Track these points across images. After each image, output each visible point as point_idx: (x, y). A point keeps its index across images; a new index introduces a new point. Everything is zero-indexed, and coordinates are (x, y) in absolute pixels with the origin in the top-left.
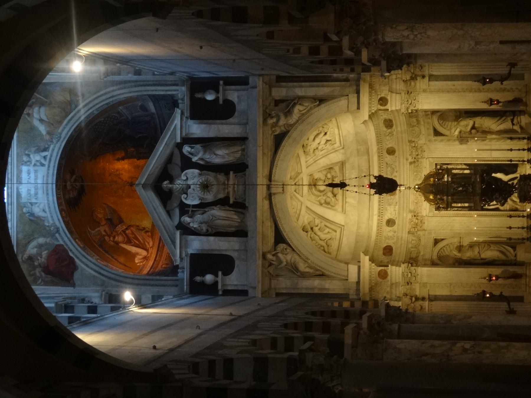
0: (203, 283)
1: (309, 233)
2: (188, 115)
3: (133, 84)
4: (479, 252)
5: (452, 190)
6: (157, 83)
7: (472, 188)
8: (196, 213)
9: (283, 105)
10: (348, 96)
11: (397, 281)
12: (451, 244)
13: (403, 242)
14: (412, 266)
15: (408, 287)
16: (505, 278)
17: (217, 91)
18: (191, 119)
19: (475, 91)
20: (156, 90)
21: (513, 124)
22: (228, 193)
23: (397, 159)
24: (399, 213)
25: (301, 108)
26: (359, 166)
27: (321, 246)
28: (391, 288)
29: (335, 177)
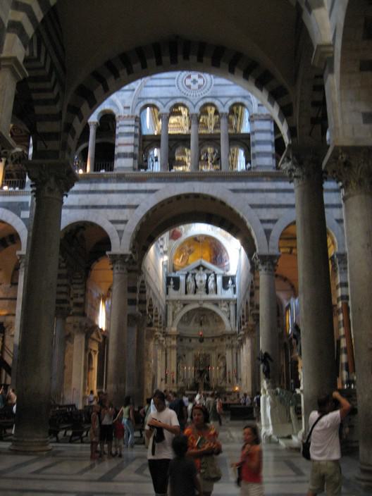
9: (227, 306)
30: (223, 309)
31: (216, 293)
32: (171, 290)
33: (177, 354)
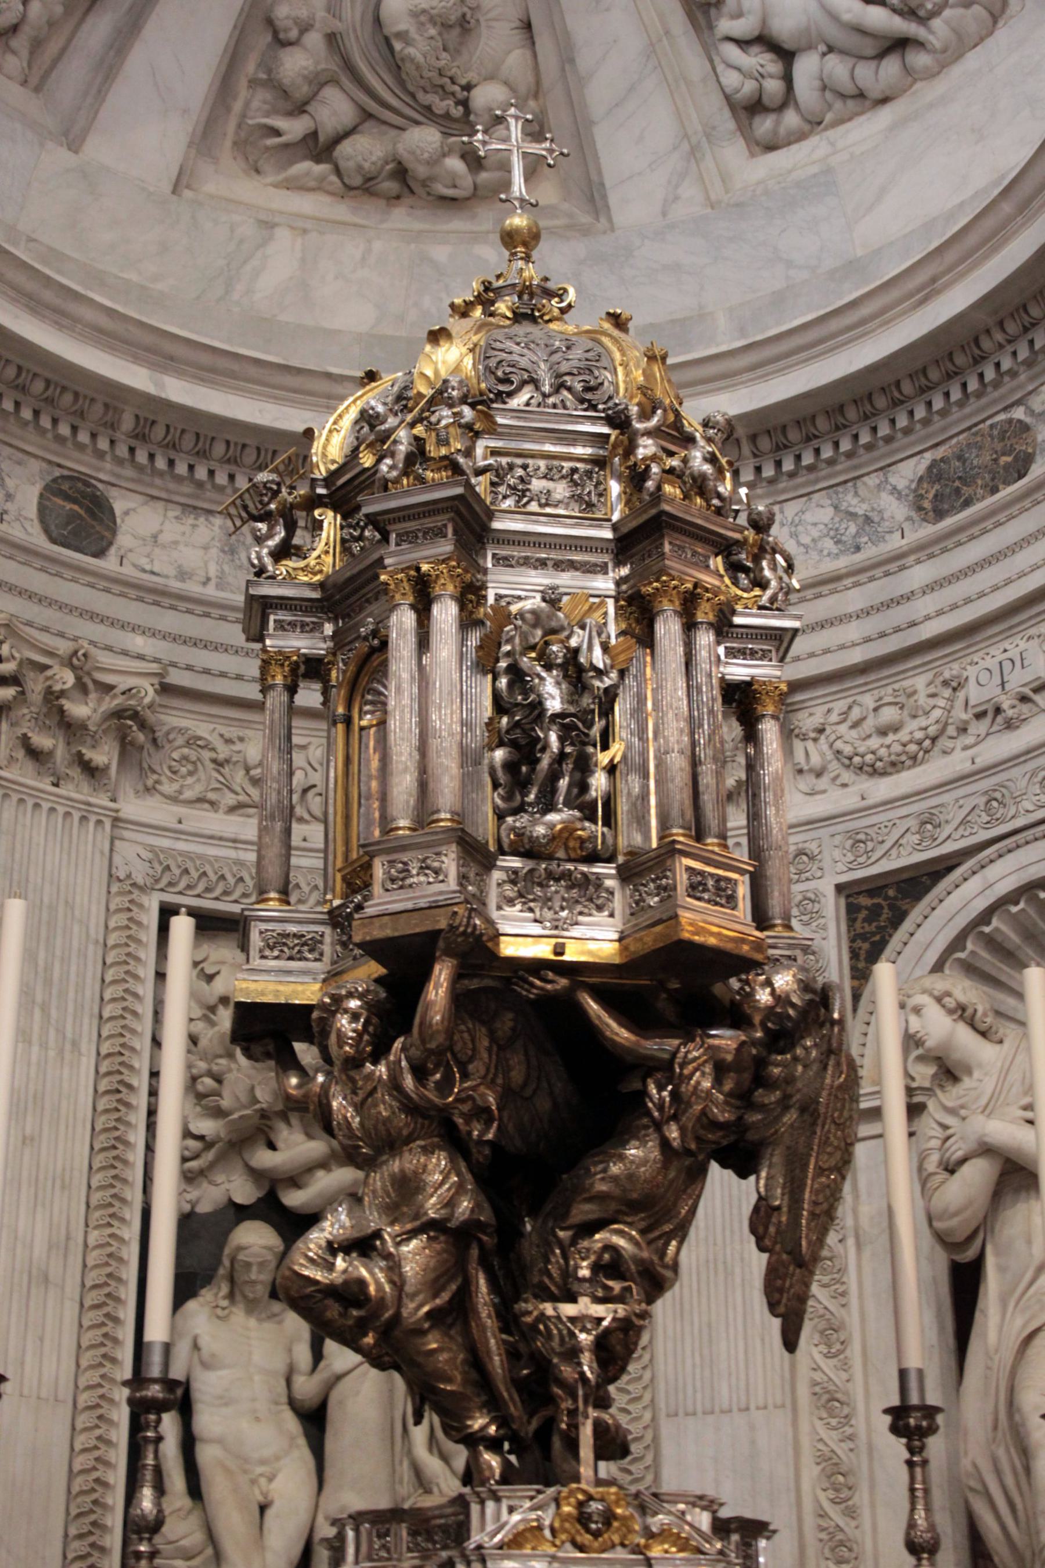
5: (535, 602)
24: (158, 595)
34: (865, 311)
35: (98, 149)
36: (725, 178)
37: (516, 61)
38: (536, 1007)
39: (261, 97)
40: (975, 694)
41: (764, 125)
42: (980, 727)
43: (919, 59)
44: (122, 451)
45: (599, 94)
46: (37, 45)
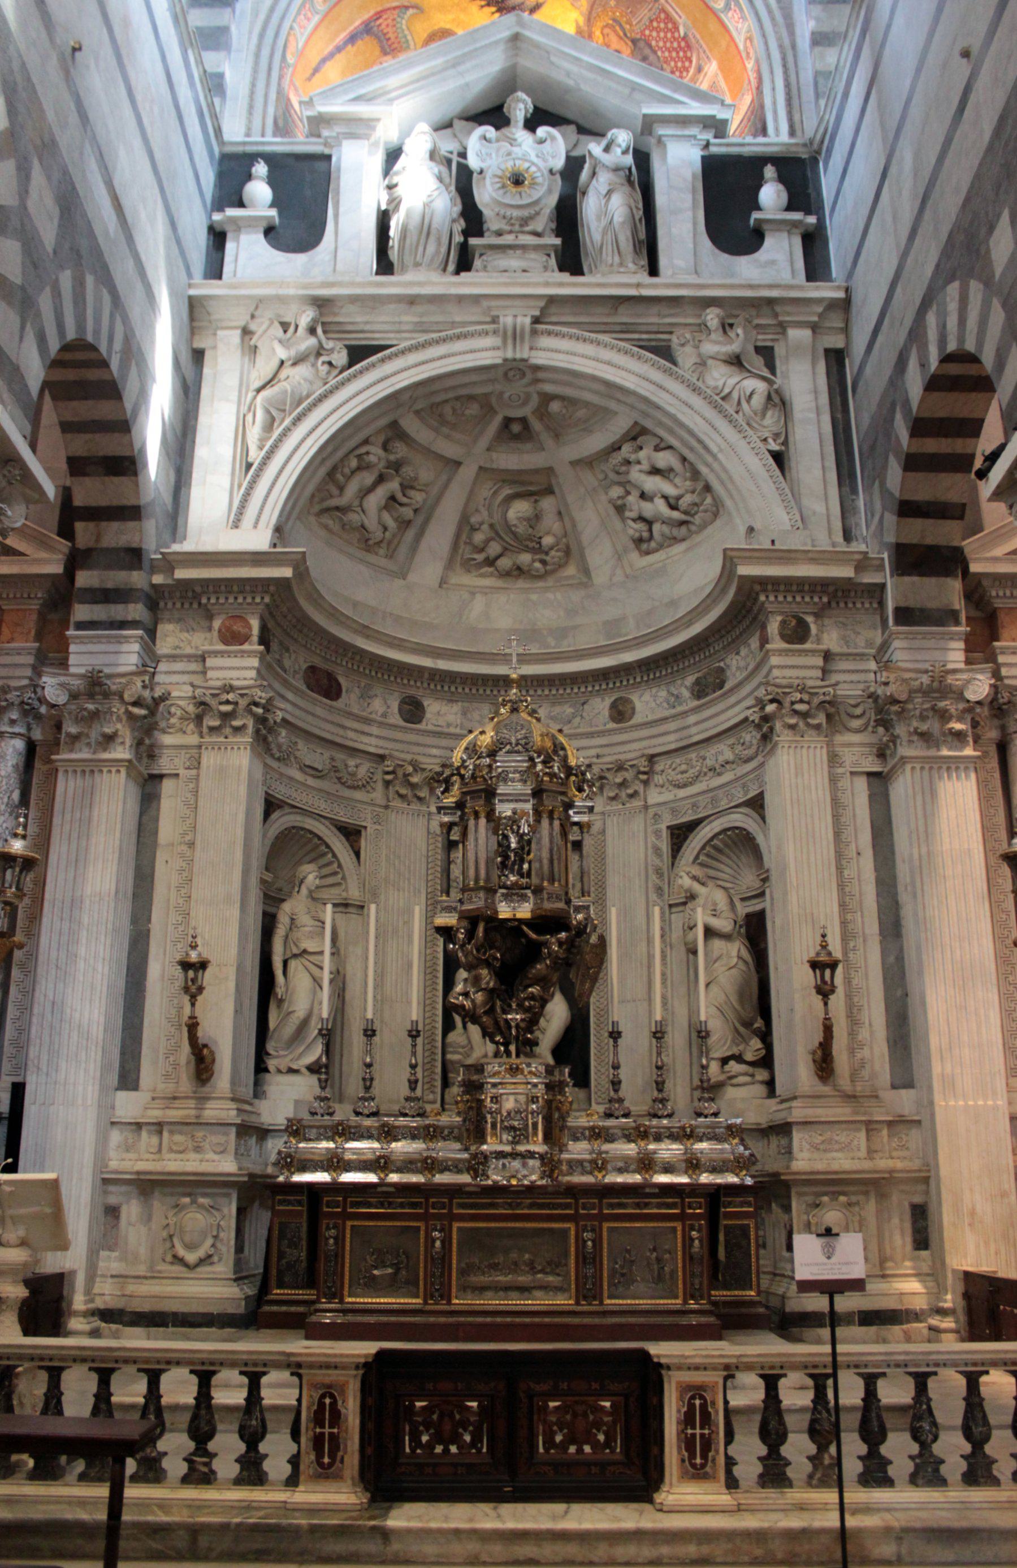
0: (249, 177)
1: (380, 452)
2: (714, 150)
3: (787, 42)
4: (305, 951)
5: (509, 813)
6: (794, 91)
7: (515, 885)
8: (444, 170)
10: (805, 528)
11: (210, 674)
12: (344, 878)
13: (351, 734)
14: (261, 720)
15: (191, 708)
16: (192, 1017)
17: (789, 208)
18: (703, 158)
19: (844, 923)
20: (774, 89)
21: (724, 1061)
22: (499, 234)
23: (601, 728)
25: (758, 401)
26: (575, 627)
27: (341, 489)
28: (189, 657)
29: (544, 562)
30: (721, 377)
31: (653, 270)
32: (250, 256)
33: (271, 806)
34: (671, 628)
35: (412, 577)
36: (631, 566)
37: (556, 527)
38: (513, 928)
39: (468, 548)
40: (709, 762)
41: (644, 546)
42: (711, 774)
43: (693, 528)
44: (425, 685)
45: (585, 539)
46: (389, 543)
